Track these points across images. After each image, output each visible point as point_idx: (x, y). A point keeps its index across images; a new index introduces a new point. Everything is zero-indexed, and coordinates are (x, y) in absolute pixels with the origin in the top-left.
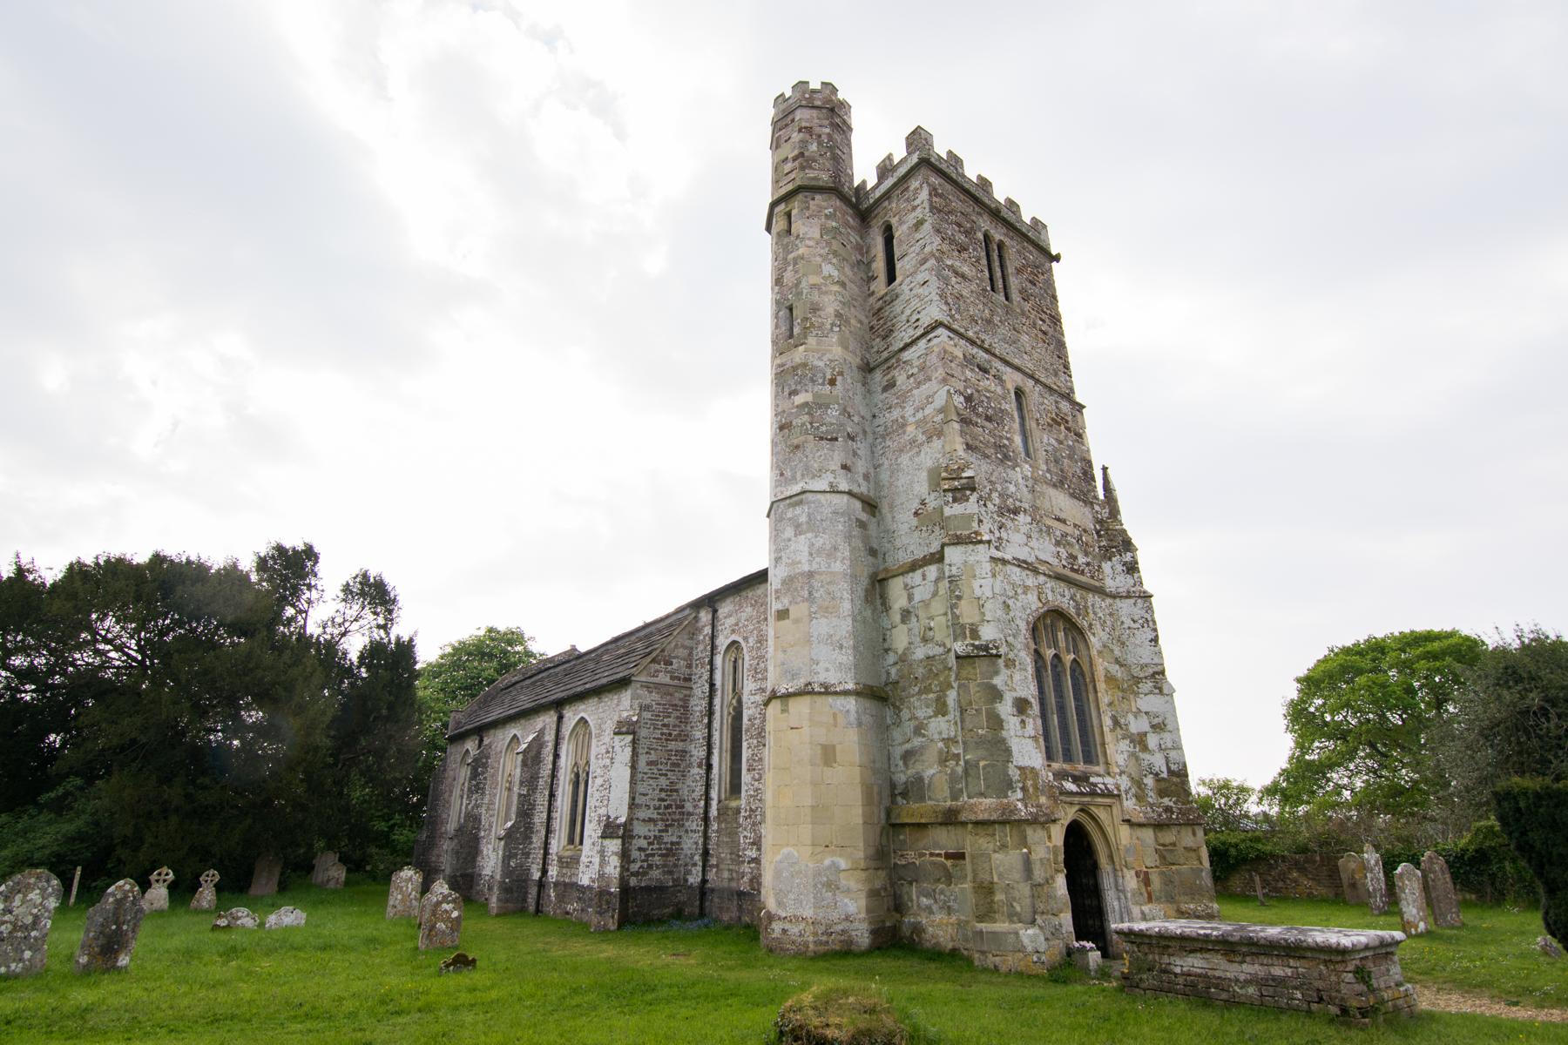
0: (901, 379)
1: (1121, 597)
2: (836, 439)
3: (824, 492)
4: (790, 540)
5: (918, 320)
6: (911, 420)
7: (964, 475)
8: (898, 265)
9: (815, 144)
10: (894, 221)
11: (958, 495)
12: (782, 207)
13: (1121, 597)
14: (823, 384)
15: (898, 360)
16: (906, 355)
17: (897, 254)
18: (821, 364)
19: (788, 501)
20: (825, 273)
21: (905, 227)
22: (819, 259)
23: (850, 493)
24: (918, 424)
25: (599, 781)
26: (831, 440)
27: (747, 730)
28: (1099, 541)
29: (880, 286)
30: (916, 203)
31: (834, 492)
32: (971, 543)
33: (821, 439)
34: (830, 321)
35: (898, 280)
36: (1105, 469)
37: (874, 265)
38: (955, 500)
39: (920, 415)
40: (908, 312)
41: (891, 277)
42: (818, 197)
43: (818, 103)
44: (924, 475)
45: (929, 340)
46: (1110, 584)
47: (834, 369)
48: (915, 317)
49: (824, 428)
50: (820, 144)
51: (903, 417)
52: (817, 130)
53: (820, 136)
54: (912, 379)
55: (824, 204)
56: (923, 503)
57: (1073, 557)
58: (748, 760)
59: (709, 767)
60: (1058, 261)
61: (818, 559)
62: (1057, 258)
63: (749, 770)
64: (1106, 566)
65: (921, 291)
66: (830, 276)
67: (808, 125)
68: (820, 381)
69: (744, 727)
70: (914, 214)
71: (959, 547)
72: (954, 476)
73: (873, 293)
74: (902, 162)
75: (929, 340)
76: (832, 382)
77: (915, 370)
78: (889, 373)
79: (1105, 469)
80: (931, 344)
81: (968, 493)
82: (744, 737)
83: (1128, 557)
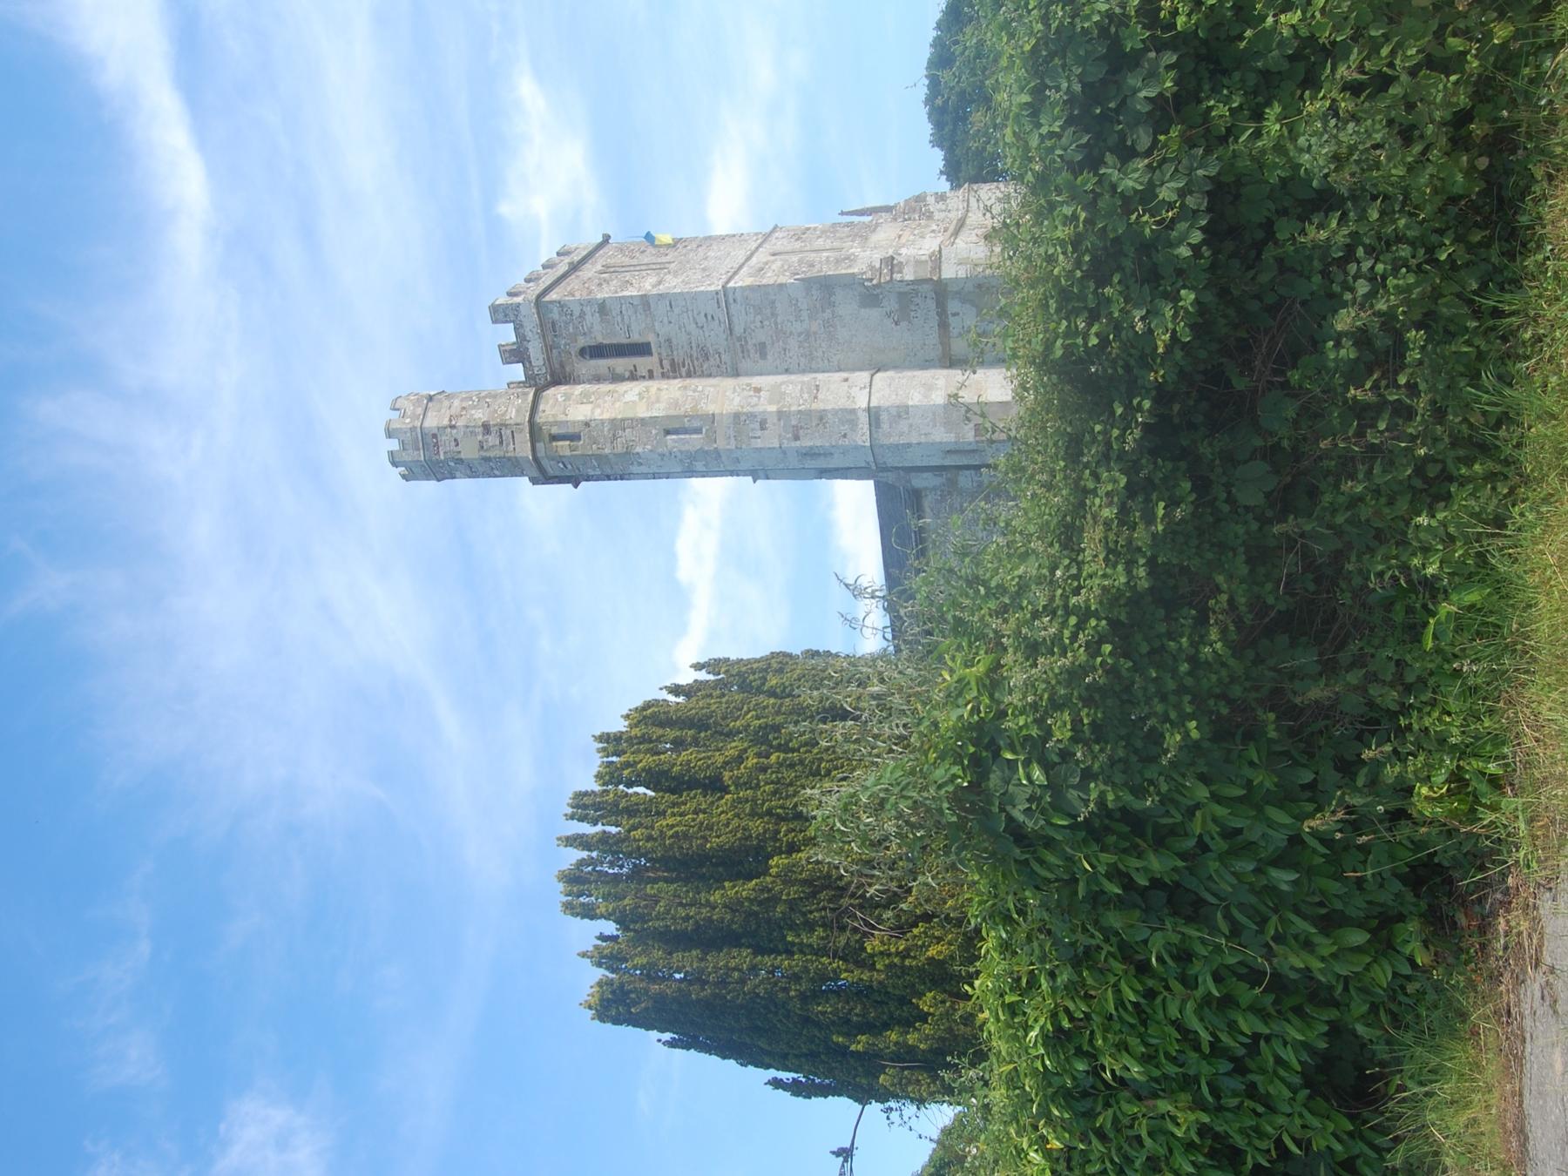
0: (761, 336)
1: (968, 206)
2: (817, 386)
3: (870, 392)
4: (911, 426)
5: (706, 315)
7: (878, 266)
8: (636, 338)
9: (473, 412)
10: (582, 342)
11: (896, 269)
12: (540, 446)
13: (968, 206)
14: (759, 397)
15: (739, 339)
16: (738, 330)
18: (737, 400)
19: (873, 428)
20: (636, 398)
21: (597, 327)
22: (617, 405)
23: (872, 376)
26: (818, 390)
28: (915, 220)
29: (643, 363)
30: (577, 313)
31: (870, 386)
32: (940, 258)
33: (816, 397)
34: (691, 393)
35: (651, 338)
36: (842, 213)
37: (619, 370)
38: (901, 272)
39: (805, 314)
41: (642, 349)
42: (541, 407)
43: (420, 411)
44: (864, 312)
45: (734, 300)
46: (955, 216)
47: (743, 389)
48: (701, 320)
49: (806, 396)
50: (474, 407)
52: (453, 411)
53: (464, 408)
55: (551, 402)
57: (933, 231)
60: (609, 237)
61: (933, 396)
62: (606, 239)
64: (937, 216)
65: (677, 310)
66: (640, 394)
67: (447, 419)
68: (756, 399)
70: (588, 317)
71: (943, 268)
72: (878, 274)
73: (651, 372)
74: (518, 330)
76: (757, 390)
77: (759, 318)
78: (748, 351)
79: (842, 213)
80: (739, 299)
81: (895, 262)
83: (930, 200)
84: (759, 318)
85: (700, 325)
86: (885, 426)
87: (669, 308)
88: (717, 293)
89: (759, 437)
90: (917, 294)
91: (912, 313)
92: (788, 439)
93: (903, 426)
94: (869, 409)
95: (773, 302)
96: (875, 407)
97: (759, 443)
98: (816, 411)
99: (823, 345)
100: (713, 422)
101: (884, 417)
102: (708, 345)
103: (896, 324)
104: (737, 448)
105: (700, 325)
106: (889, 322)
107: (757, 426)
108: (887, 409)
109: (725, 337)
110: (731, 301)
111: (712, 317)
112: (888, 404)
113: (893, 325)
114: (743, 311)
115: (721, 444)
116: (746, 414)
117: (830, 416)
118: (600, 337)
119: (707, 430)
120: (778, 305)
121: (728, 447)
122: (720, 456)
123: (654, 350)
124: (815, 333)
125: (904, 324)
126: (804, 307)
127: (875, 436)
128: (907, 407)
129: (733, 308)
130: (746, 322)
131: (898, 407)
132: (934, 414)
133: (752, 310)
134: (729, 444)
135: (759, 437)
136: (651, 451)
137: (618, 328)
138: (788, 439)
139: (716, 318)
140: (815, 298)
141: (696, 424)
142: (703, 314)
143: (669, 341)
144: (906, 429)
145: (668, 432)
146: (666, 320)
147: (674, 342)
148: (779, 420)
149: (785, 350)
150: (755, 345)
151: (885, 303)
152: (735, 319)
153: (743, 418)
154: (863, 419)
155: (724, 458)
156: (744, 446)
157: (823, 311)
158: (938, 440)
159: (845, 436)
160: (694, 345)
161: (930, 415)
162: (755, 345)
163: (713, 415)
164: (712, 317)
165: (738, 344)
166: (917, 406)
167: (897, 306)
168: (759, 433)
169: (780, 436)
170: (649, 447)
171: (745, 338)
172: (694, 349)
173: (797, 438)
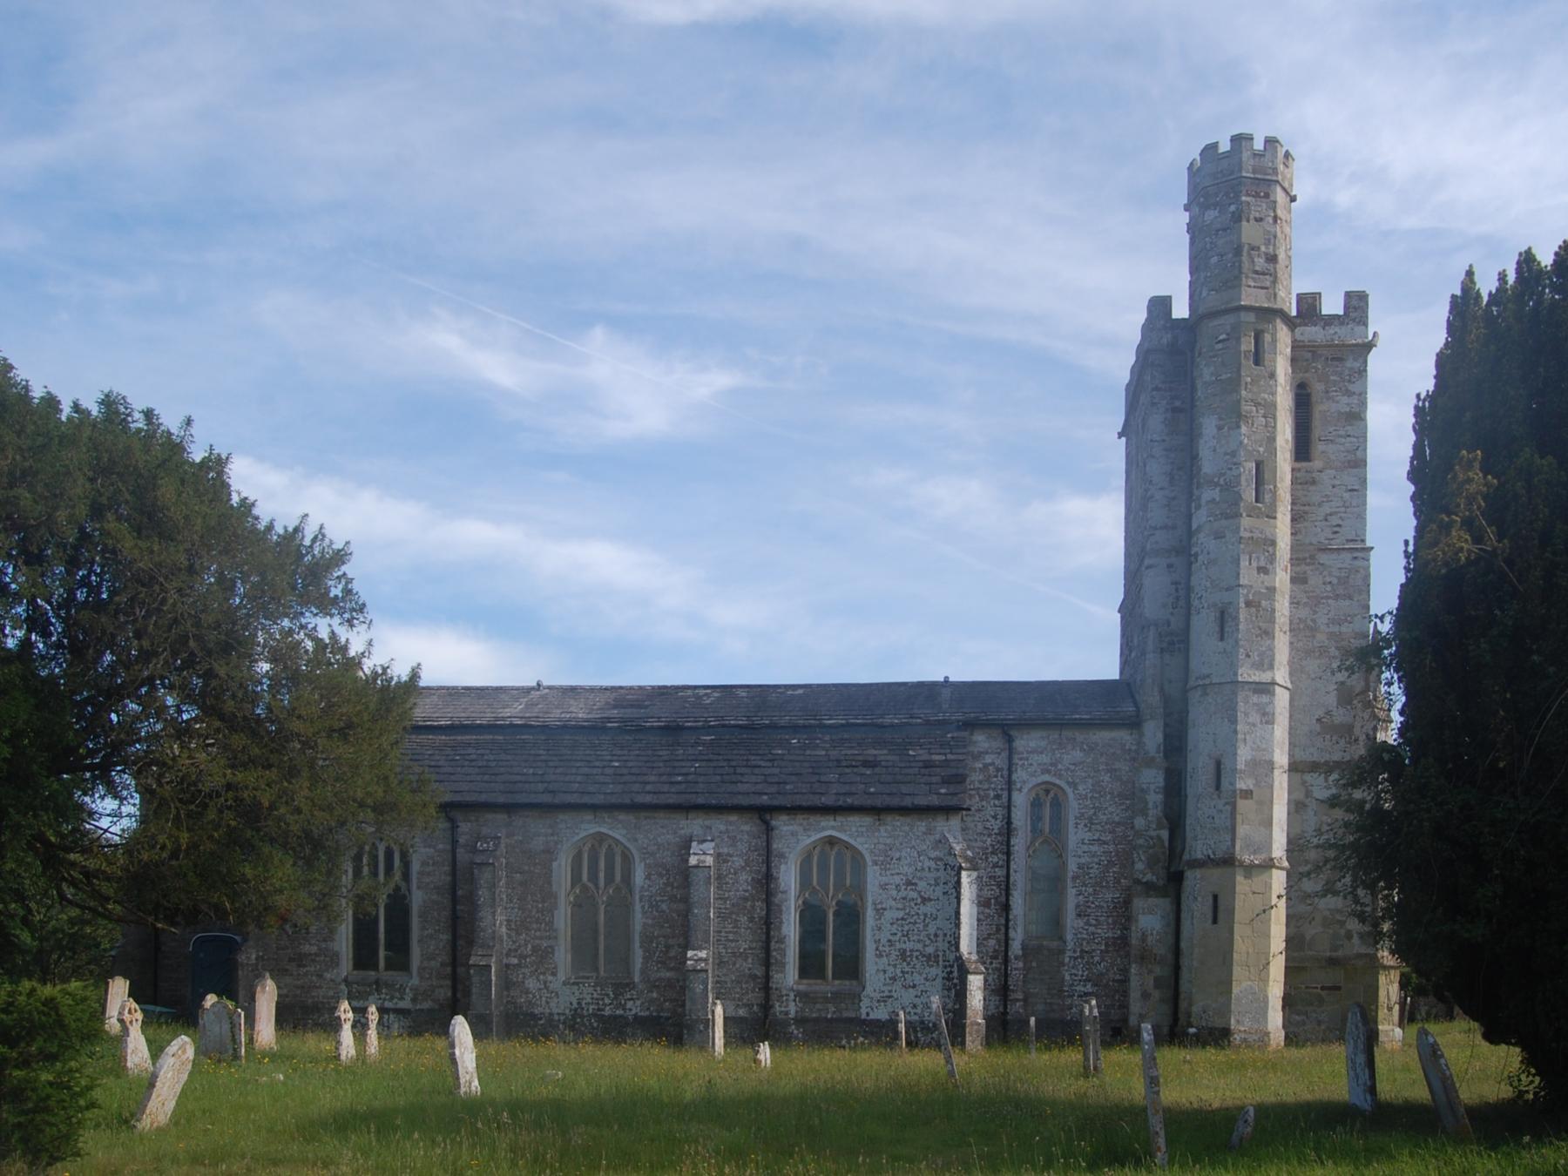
0: (1315, 581)
4: (1254, 725)
5: (1339, 526)
6: (1323, 627)
8: (1318, 448)
15: (1312, 557)
16: (1323, 558)
17: (1318, 430)
19: (1254, 686)
24: (1331, 635)
25: (889, 915)
27: (1075, 878)
35: (1317, 464)
39: (1336, 629)
40: (1326, 509)
45: (1355, 558)
48: (1335, 520)
51: (1314, 621)
54: (1329, 588)
56: (1328, 713)
58: (1077, 906)
59: (1006, 908)
63: (1079, 915)
65: (1347, 495)
69: (1070, 874)
75: (1355, 558)
77: (1335, 581)
78: (1298, 565)
82: (1069, 883)
84: (1335, 581)
85: (1329, 517)
86: (1255, 699)
87: (1349, 488)
88: (1363, 541)
89: (1250, 564)
90: (1350, 743)
91: (1328, 736)
92: (1247, 595)
93: (1255, 717)
94: (1274, 683)
95: (1350, 598)
96: (1274, 690)
97: (1244, 563)
98: (1274, 629)
99: (1301, 644)
100: (1268, 517)
101: (1265, 699)
102: (1306, 524)
103: (1318, 720)
104: (1241, 538)
105: (1329, 517)
106: (1320, 713)
107: (1262, 564)
108: (1271, 702)
109: (1315, 542)
110: (1355, 555)
111: (1336, 532)
112: (1276, 703)
113: (1317, 717)
114: (1343, 566)
115: (1246, 522)
116: (1274, 554)
117: (1269, 642)
118: (1320, 409)
119: (1260, 509)
120: (1347, 602)
121: (1242, 529)
122: (1226, 518)
123: (1304, 464)
124: (1314, 637)
125: (1318, 728)
126: (1344, 629)
127: (1246, 687)
128: (1273, 723)
129: (1347, 556)
130: (1330, 567)
131: (1274, 714)
132: (1264, 750)
133: (1343, 574)
134: (1245, 529)
135: (1250, 564)
136: (1241, 443)
137: (1331, 429)
138: (1247, 595)
139: (1335, 536)
140: (1352, 640)
141: (1267, 497)
142: (1340, 522)
143: (1314, 482)
144: (1251, 720)
145: (1258, 465)
146: (1337, 482)
147: (1312, 488)
148: (1267, 588)
149: (1298, 603)
150: (1305, 572)
151: (1341, 711)
152: (1334, 556)
153: (1270, 549)
154: (1265, 677)
155: (1224, 522)
156: (1242, 546)
157: (1337, 648)
158: (1239, 752)
159: (1248, 656)
160: (1307, 508)
161: (1264, 746)
162: (1305, 572)
163: (1275, 518)
164: (1336, 532)
165: (1307, 555)
166: (1273, 732)
167: (1336, 722)
168: (1254, 564)
169: (1251, 586)
170: (1246, 441)
171: (1313, 564)
172: (1302, 508)
173: (1248, 604)
